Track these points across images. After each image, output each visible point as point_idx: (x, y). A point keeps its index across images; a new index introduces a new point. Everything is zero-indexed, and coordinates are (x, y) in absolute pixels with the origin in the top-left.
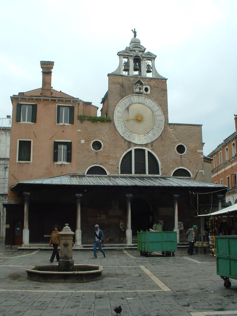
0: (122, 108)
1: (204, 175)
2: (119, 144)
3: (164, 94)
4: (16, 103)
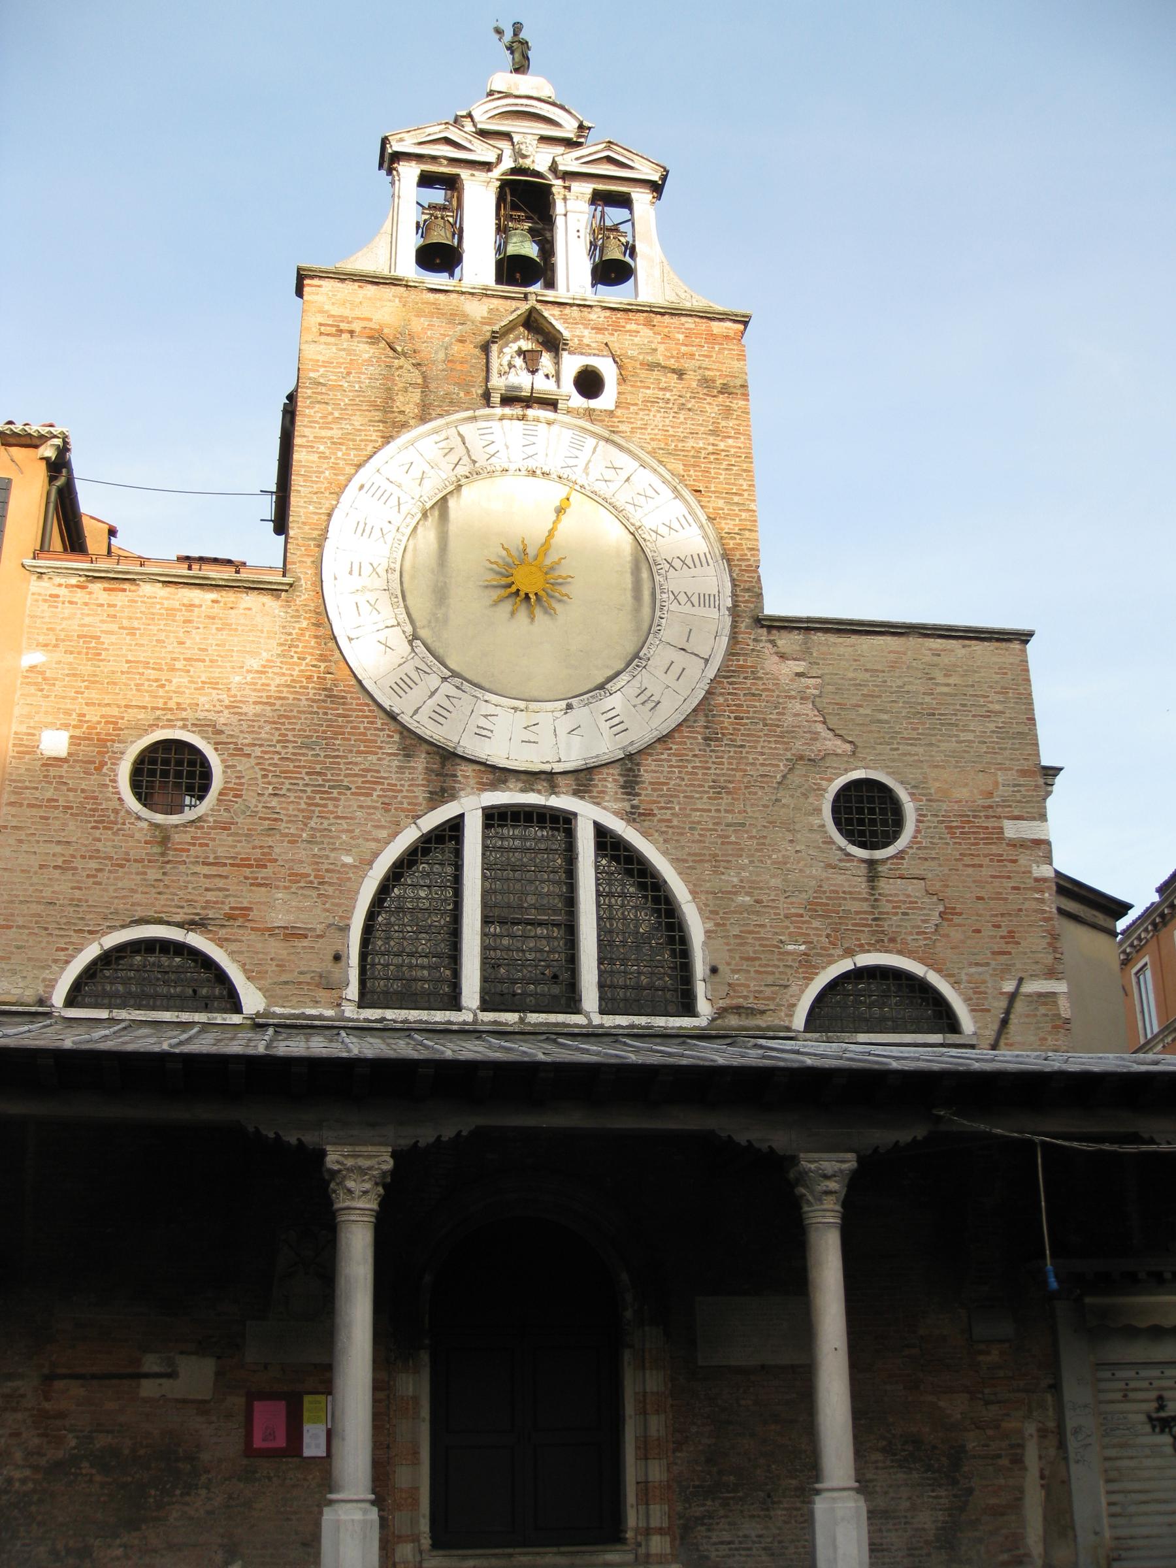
0: (393, 501)
1: (1067, 1021)
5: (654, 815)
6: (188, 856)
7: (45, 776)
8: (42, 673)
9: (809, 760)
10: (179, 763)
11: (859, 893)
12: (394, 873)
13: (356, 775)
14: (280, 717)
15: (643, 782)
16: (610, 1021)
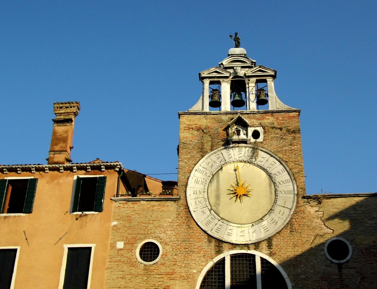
0: (204, 173)
2: (196, 247)
5: (277, 254)
6: (154, 273)
7: (118, 254)
8: (117, 227)
9: (320, 235)
11: (336, 273)
12: (207, 274)
13: (196, 248)
14: (177, 234)
15: (273, 245)
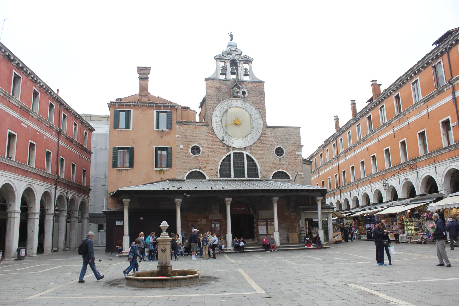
1: (303, 177)
3: (262, 97)
4: (113, 109)
10: (196, 148)
16: (249, 179)
